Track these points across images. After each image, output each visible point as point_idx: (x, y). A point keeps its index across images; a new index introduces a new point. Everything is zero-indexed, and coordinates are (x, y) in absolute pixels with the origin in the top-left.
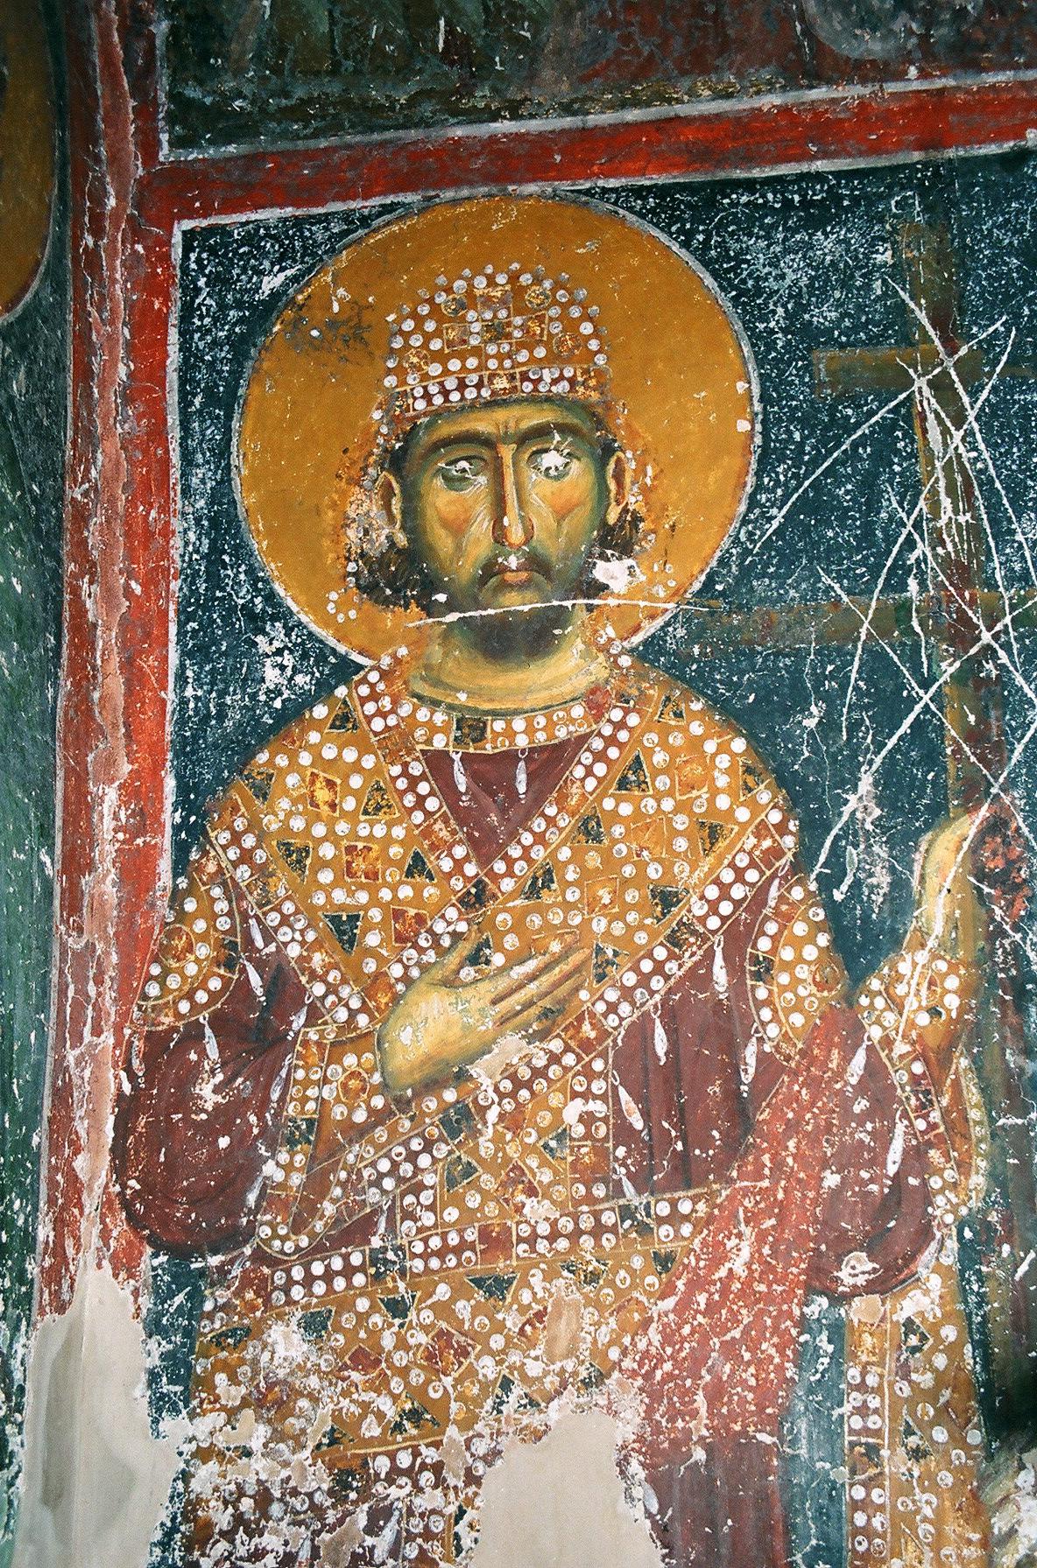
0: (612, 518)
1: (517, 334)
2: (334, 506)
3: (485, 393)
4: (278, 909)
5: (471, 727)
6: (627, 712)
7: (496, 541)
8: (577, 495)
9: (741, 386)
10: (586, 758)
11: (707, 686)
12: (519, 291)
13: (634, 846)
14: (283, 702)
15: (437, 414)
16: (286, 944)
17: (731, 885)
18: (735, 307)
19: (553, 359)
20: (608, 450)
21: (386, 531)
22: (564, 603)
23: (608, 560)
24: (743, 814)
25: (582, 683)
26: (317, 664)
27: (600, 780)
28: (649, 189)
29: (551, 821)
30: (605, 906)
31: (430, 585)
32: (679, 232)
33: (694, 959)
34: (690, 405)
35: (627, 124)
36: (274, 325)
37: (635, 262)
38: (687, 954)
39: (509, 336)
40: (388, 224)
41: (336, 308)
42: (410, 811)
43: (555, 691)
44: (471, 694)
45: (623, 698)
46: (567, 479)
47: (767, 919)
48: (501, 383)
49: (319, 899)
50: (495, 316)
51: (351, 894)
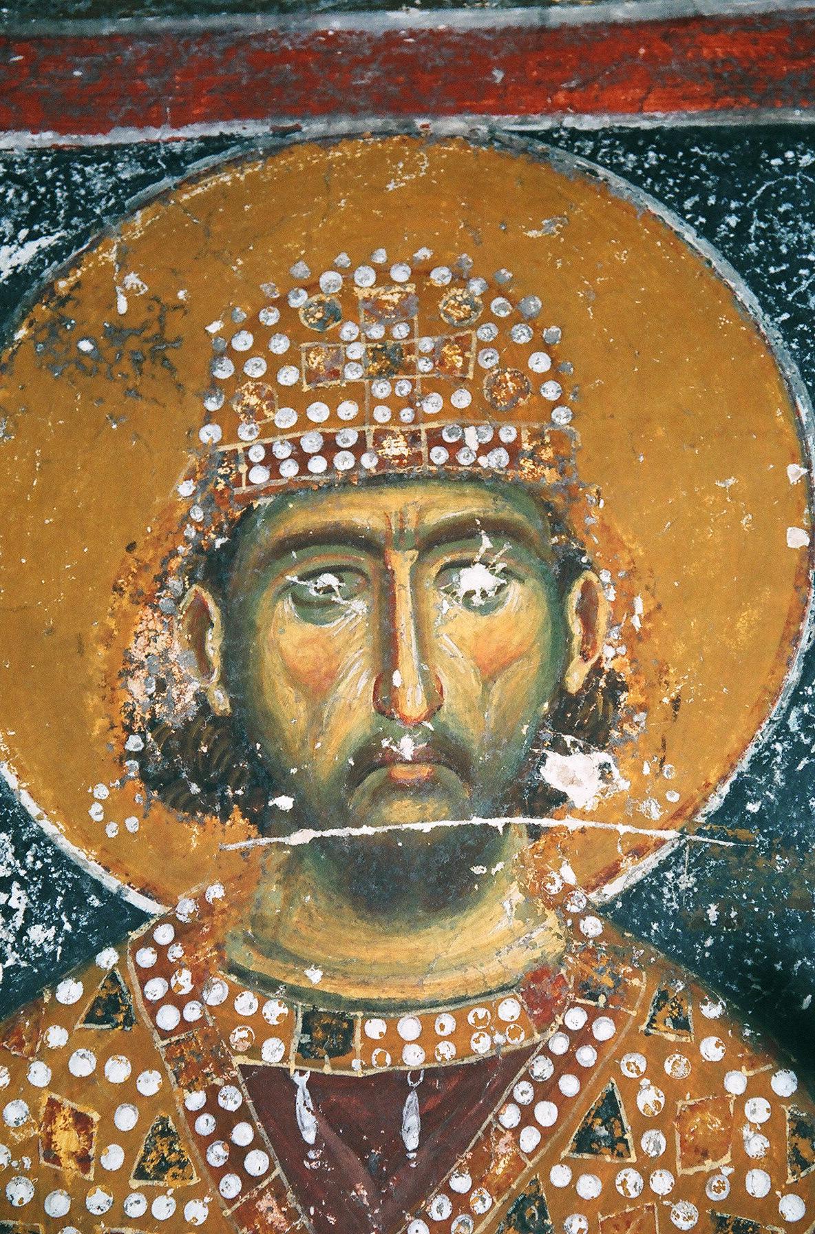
0: (576, 679)
1: (424, 366)
2: (107, 639)
3: (369, 462)
5: (328, 1028)
6: (593, 1014)
7: (380, 711)
8: (517, 639)
10: (523, 1092)
12: (428, 296)
15: (287, 493)
19: (484, 410)
20: (567, 569)
21: (194, 686)
22: (492, 822)
23: (566, 752)
25: (518, 961)
26: (67, 907)
27: (546, 1133)
28: (649, 135)
29: (460, 1202)
31: (267, 779)
32: (696, 209)
34: (709, 499)
35: (614, 26)
36: (17, 328)
37: (623, 257)
39: (410, 368)
40: (214, 170)
41: (122, 305)
42: (218, 1174)
43: (472, 974)
44: (329, 972)
45: (588, 990)
46: (500, 612)
48: (396, 447)
50: (388, 335)
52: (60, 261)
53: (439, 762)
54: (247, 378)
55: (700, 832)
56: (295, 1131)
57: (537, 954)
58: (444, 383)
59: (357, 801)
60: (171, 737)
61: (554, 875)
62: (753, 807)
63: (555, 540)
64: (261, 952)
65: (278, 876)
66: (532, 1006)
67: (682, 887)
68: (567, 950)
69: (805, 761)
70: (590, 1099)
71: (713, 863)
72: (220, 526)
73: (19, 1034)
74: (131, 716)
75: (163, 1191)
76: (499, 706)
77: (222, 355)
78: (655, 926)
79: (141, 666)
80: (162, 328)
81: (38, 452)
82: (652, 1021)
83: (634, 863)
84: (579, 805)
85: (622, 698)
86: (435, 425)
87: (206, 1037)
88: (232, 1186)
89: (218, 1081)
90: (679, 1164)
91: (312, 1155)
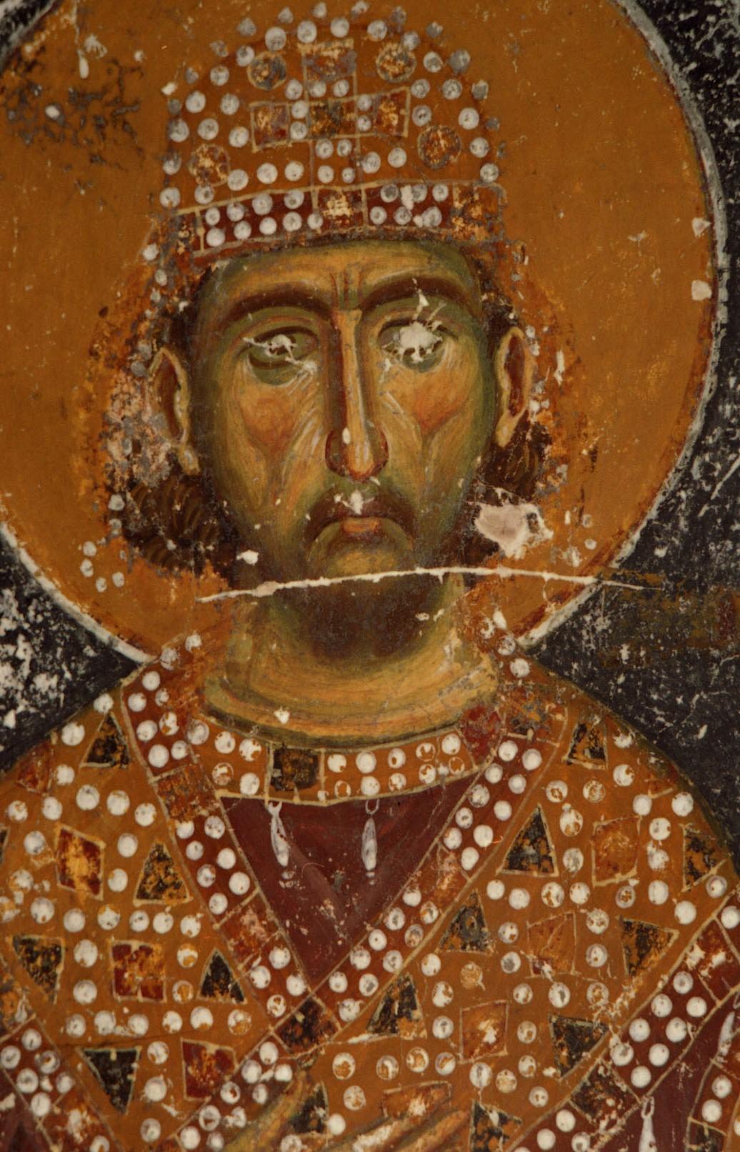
0: (504, 435)
1: (363, 124)
2: (87, 403)
3: (315, 222)
4: (16, 1042)
5: (293, 764)
6: (523, 747)
7: (332, 467)
8: (451, 397)
9: (698, 225)
10: (464, 817)
11: (639, 709)
13: (531, 957)
14: (19, 717)
15: (239, 254)
16: (29, 1097)
17: (667, 1019)
18: (694, 89)
19: (417, 171)
21: (167, 446)
23: (498, 503)
24: (686, 913)
25: (459, 700)
26: (67, 657)
29: (412, 914)
30: (488, 1047)
31: (233, 538)
33: (613, 1131)
34: (623, 254)
38: (603, 1124)
39: (350, 127)
41: (84, 69)
42: (208, 893)
43: (419, 712)
45: (518, 725)
46: (437, 369)
47: (716, 1073)
48: (339, 208)
49: (77, 1028)
50: (329, 92)
51: (122, 1020)
52: (25, 23)
53: (385, 516)
54: (200, 140)
55: (615, 577)
56: (271, 855)
57: (474, 693)
58: (380, 143)
59: (315, 553)
60: (147, 496)
61: (487, 620)
62: (660, 553)
63: (485, 297)
64: (235, 696)
65: (246, 626)
66: (471, 740)
67: (599, 629)
68: (500, 690)
69: (705, 508)
70: (520, 822)
71: (625, 606)
72: (182, 290)
73: (32, 772)
74: (111, 476)
75: (162, 909)
76: (436, 461)
77: (177, 117)
78: (575, 666)
79: (118, 428)
80: (121, 91)
81: (15, 219)
82: (573, 751)
83: (557, 608)
84: (509, 554)
85: (546, 451)
86: (373, 185)
87: (192, 772)
88: (219, 903)
89: (204, 813)
90: (594, 878)
91: (286, 876)
